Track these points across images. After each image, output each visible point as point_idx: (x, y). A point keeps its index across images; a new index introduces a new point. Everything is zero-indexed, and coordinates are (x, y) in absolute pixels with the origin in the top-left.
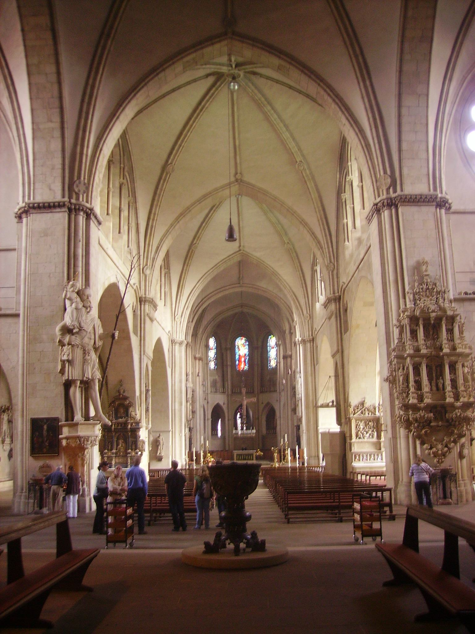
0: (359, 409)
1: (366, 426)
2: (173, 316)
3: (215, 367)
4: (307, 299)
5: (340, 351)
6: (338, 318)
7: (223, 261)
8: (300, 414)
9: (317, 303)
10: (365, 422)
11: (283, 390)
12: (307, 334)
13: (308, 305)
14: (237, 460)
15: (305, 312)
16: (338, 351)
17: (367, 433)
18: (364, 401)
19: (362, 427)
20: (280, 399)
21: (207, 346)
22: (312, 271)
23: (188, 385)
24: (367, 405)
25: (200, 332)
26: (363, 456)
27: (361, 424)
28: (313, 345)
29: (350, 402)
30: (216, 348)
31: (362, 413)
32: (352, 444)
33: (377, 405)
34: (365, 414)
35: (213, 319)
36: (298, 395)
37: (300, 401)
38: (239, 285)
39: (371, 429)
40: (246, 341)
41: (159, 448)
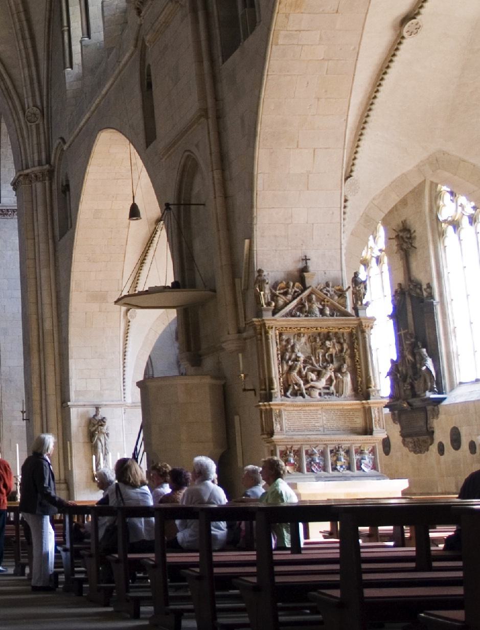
0: (289, 297)
1: (314, 351)
4: (33, 68)
5: (211, 114)
6: (201, 14)
13: (36, 85)
15: (28, 102)
16: (204, 113)
17: (319, 375)
19: (302, 357)
24: (314, 280)
27: (298, 347)
29: (260, 271)
31: (301, 308)
33: (347, 283)
39: (332, 362)
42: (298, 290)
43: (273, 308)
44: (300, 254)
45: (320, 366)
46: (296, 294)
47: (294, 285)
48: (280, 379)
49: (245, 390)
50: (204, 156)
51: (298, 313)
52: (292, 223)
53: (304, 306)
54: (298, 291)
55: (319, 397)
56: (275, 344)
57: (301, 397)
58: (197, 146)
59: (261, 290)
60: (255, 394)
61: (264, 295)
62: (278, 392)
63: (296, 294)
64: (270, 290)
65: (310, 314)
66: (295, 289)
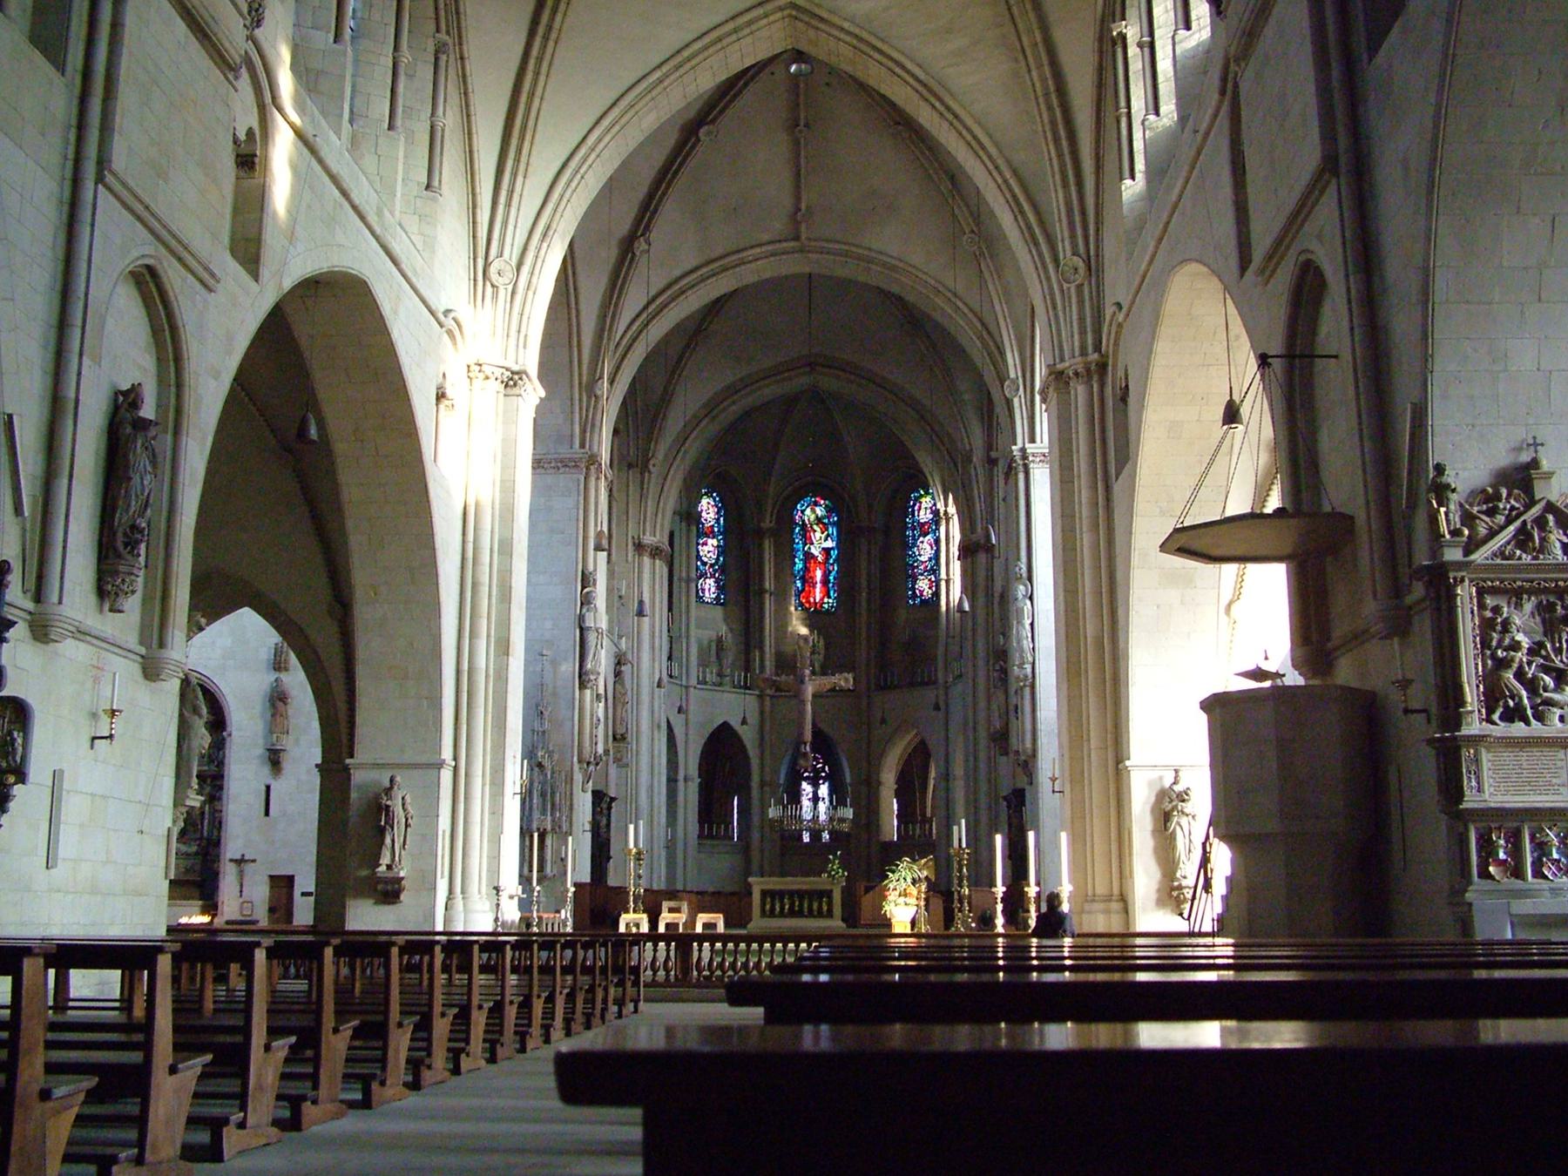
0: (1501, 519)
2: (480, 262)
3: (717, 598)
4: (1073, 188)
7: (706, 40)
8: (1028, 745)
9: (1128, 182)
10: (1544, 610)
11: (960, 676)
12: (1071, 342)
13: (1077, 219)
14: (763, 913)
15: (1064, 249)
16: (1329, 165)
18: (1534, 463)
19: (1525, 642)
20: (947, 705)
21: (690, 516)
22: (1101, 40)
23: (589, 623)
25: (660, 456)
26: (1541, 848)
28: (1102, 392)
29: (1440, 469)
30: (726, 532)
31: (1522, 539)
32: (1467, 753)
34: (1542, 550)
35: (711, 408)
36: (1021, 666)
37: (1027, 691)
38: (792, 244)
40: (829, 510)
41: (388, 841)
42: (1517, 505)
43: (1465, 539)
44: (1519, 434)
45: (1562, 661)
46: (1514, 513)
47: (1509, 495)
48: (1478, 686)
49: (1406, 711)
50: (1331, 259)
51: (1518, 552)
52: (1505, 370)
53: (1530, 537)
54: (1518, 509)
55: (1559, 725)
56: (1470, 616)
57: (1522, 724)
58: (1319, 237)
59: (1440, 505)
60: (1429, 721)
61: (1447, 514)
62: (1473, 712)
63: (1514, 513)
64: (1461, 505)
65: (1543, 554)
66: (1513, 502)
